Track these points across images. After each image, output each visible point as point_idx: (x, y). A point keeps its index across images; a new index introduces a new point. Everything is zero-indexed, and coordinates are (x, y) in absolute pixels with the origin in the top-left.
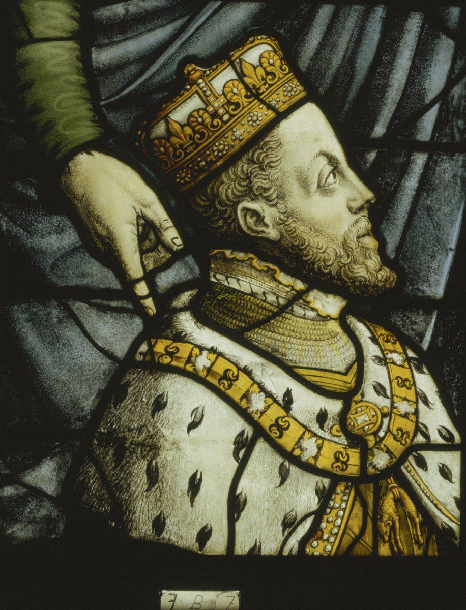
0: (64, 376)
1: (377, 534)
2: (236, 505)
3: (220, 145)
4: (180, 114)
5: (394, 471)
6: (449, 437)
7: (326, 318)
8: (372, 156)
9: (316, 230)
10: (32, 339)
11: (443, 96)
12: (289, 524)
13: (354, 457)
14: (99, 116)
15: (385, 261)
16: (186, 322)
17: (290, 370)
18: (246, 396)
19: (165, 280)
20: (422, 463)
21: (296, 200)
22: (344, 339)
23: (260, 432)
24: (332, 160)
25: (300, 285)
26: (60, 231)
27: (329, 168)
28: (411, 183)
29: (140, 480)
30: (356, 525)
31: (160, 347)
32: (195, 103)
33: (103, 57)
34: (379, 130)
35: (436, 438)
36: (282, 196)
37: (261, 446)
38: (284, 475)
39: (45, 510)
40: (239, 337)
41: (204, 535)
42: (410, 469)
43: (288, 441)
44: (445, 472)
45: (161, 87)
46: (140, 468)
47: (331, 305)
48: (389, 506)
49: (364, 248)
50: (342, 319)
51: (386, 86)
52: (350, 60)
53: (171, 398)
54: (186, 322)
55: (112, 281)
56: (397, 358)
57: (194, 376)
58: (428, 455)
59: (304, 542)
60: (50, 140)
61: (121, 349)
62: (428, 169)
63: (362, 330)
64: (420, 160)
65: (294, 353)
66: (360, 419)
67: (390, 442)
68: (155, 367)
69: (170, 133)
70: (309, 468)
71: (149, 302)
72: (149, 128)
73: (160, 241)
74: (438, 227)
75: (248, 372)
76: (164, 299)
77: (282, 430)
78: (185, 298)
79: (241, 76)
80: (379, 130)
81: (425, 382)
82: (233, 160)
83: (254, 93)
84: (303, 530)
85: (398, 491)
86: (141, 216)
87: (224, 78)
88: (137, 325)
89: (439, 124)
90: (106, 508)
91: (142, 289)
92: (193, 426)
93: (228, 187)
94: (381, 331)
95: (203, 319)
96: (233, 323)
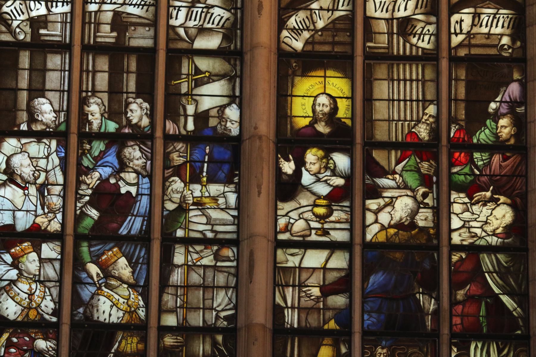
0: (84, 295)
1: (132, 320)
2: (110, 315)
3: (109, 262)
4: (103, 258)
5: (135, 311)
6: (143, 306)
7: (125, 288)
8: (132, 265)
9: (124, 275)
10: (80, 290)
11: (143, 257)
12: (118, 318)
13: (129, 309)
14: (91, 258)
15: (134, 280)
16: (103, 288)
17: (119, 295)
18: (112, 299)
19: (100, 282)
20: (139, 310)
21: (121, 271)
22: (128, 291)
23: (114, 304)
24: (126, 265)
25: (121, 283)
26: (84, 274)
27: (126, 266)
28: (138, 269)
29: (95, 311)
30: (129, 319)
31: (99, 291)
32: (106, 256)
33: (92, 249)
34: (134, 261)
35: (141, 306)
36: (119, 270)
37: (114, 307)
38: (118, 311)
39: (81, 315)
40: (111, 290)
41: (105, 320)
42: (137, 310)
43: (119, 306)
44: (143, 311)
45: (101, 254)
46: (95, 309)
47: (126, 286)
48: (134, 316)
49: (131, 278)
50: (127, 288)
51: (135, 255)
52: (129, 251)
53: (101, 299)
54: (103, 288)
55: (92, 281)
56: (136, 294)
57: (105, 296)
58: (140, 309)
59: (120, 321)
60: (84, 261)
61: (93, 292)
62: (141, 267)
63: (130, 290)
64: (140, 265)
65: (120, 293)
66: (130, 303)
67: (134, 306)
68: (98, 294)
69: (102, 260)
70: (122, 310)
71: (98, 285)
72: (99, 260)
73: (100, 276)
74: (142, 275)
75: (113, 295)
76: (100, 285)
77: (118, 304)
78: (103, 284)
79: (113, 253)
80: (134, 261)
81: (140, 298)
82: (111, 265)
83: (115, 255)
84: (120, 319)
85: (135, 314)
86: (97, 272)
87: (110, 253)
88: (96, 288)
89: (143, 261)
90: (90, 315)
91: (97, 283)
92: (104, 303)
93: (110, 268)
94: (133, 290)
95: (106, 288)
96: (111, 288)
